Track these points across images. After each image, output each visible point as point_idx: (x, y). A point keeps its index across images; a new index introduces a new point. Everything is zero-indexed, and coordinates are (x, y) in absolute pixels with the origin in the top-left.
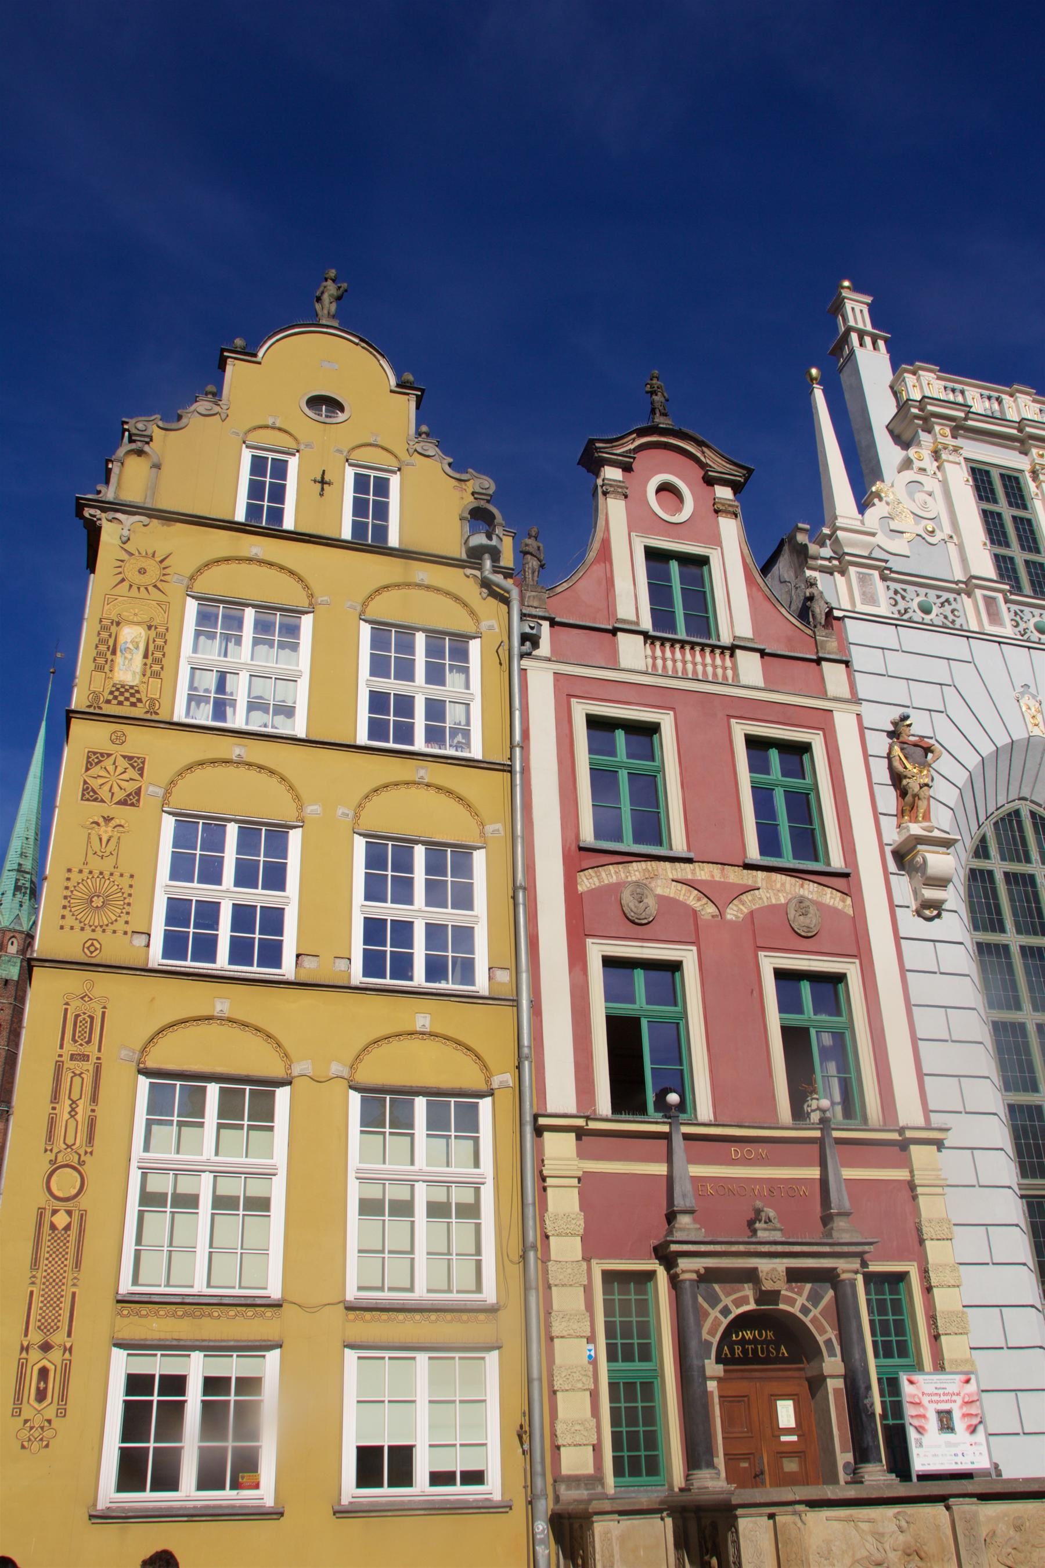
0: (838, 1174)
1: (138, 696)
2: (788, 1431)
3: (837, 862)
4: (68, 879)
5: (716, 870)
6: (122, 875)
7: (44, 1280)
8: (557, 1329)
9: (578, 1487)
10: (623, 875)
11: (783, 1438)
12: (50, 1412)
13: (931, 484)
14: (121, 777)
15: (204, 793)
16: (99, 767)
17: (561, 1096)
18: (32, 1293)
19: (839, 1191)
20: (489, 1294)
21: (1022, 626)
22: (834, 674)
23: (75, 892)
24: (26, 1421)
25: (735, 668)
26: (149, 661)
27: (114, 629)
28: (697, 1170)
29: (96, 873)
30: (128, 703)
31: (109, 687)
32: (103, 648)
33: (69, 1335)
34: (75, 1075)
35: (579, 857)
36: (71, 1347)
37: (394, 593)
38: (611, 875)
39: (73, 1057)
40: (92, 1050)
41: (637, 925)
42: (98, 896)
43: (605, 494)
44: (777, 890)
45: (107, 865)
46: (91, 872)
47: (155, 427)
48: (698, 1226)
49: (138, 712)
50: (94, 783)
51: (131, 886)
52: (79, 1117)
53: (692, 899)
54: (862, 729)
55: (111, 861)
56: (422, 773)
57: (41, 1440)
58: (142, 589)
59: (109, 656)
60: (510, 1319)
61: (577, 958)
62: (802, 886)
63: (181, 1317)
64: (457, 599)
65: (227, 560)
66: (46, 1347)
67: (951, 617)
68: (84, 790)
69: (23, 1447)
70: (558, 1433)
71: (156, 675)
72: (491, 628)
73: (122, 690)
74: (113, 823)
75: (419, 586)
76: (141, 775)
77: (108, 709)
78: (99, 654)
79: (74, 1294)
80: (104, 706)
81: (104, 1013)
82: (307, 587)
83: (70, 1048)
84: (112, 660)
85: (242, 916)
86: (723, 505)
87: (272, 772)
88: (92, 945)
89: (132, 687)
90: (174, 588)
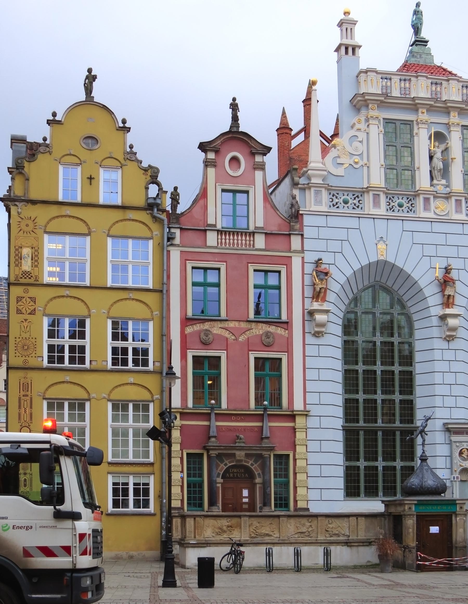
3: (284, 317)
5: (237, 324)
10: (202, 327)
15: (58, 307)
26: (33, 261)
27: (20, 250)
29: (24, 338)
31: (21, 273)
35: (186, 321)
37: (120, 224)
41: (205, 344)
44: (259, 330)
47: (25, 161)
49: (32, 281)
50: (20, 308)
53: (226, 334)
56: (131, 295)
58: (28, 233)
59: (20, 261)
62: (269, 327)
64: (144, 223)
65: (57, 217)
71: (36, 266)
72: (156, 235)
75: (130, 220)
76: (35, 304)
78: (16, 260)
80: (20, 280)
82: (87, 225)
85: (72, 349)
87: (79, 299)
89: (29, 272)
90: (39, 231)
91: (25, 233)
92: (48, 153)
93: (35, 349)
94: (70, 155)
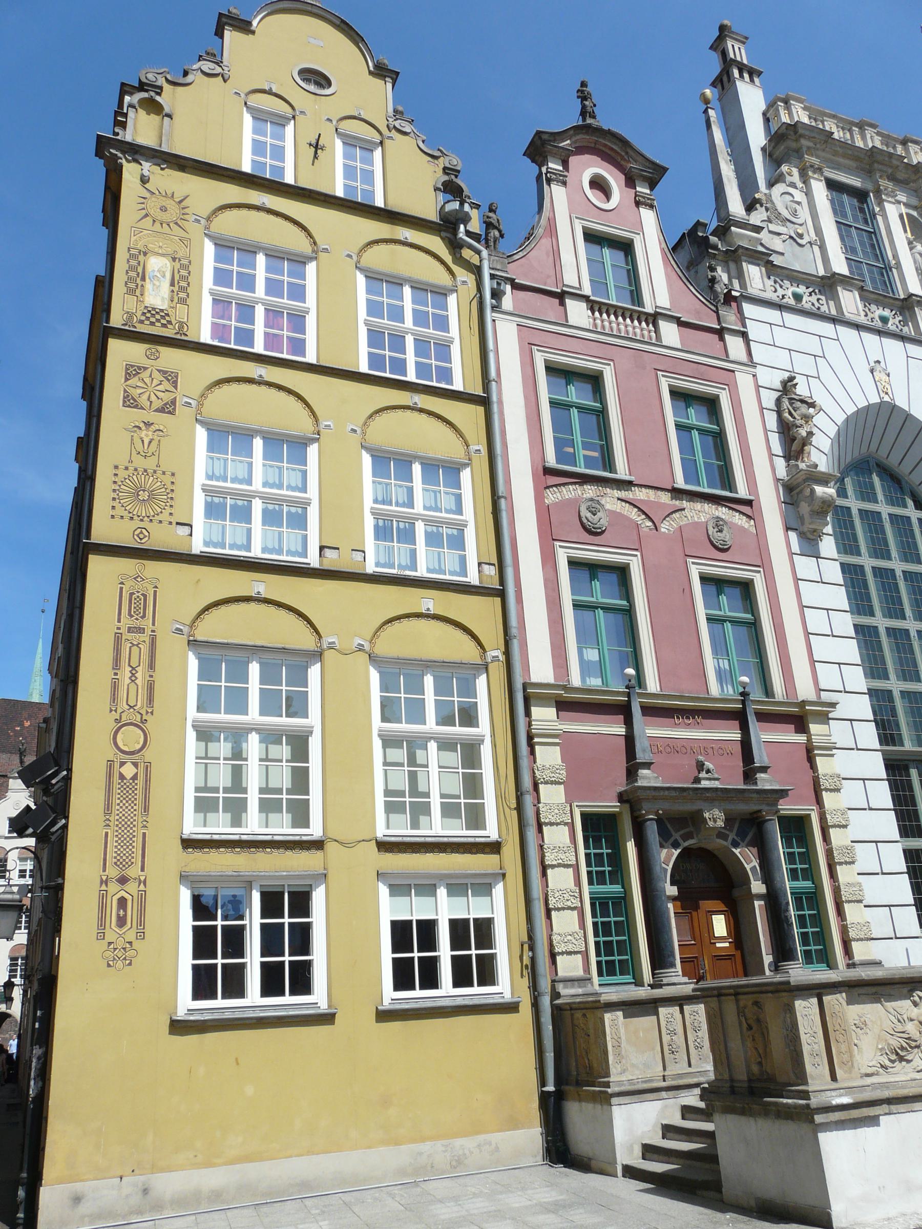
0: (758, 737)
1: (167, 318)
2: (722, 939)
3: (742, 491)
4: (116, 475)
5: (651, 492)
6: (164, 473)
7: (117, 823)
8: (550, 859)
9: (573, 987)
10: (580, 493)
11: (718, 945)
12: (131, 936)
13: (799, 196)
14: (157, 388)
16: (136, 378)
17: (541, 670)
18: (107, 834)
19: (760, 749)
20: (491, 832)
21: (870, 315)
22: (735, 345)
23: (122, 487)
24: (110, 943)
25: (657, 331)
26: (176, 289)
28: (651, 732)
29: (141, 470)
30: (159, 324)
32: (134, 274)
33: (143, 870)
34: (133, 645)
36: (145, 880)
37: (383, 247)
38: (571, 492)
39: (130, 630)
40: (147, 623)
42: (144, 491)
43: (549, 181)
45: (150, 464)
46: (136, 470)
48: (656, 775)
49: (169, 332)
50: (135, 392)
51: (173, 483)
52: (139, 682)
54: (758, 387)
55: (155, 458)
57: (125, 959)
60: (511, 851)
61: (548, 559)
63: (238, 853)
66: (123, 880)
67: (817, 305)
68: (124, 397)
69: (109, 965)
70: (555, 942)
71: (183, 301)
73: (153, 312)
74: (153, 428)
77: (141, 328)
78: (130, 279)
79: (144, 834)
81: (155, 592)
83: (126, 622)
84: (142, 286)
86: (644, 197)
87: (290, 392)
88: (141, 532)
89: (162, 310)
91: (158, 224)
92: (220, 78)
93: (170, 502)
94: (269, 92)
